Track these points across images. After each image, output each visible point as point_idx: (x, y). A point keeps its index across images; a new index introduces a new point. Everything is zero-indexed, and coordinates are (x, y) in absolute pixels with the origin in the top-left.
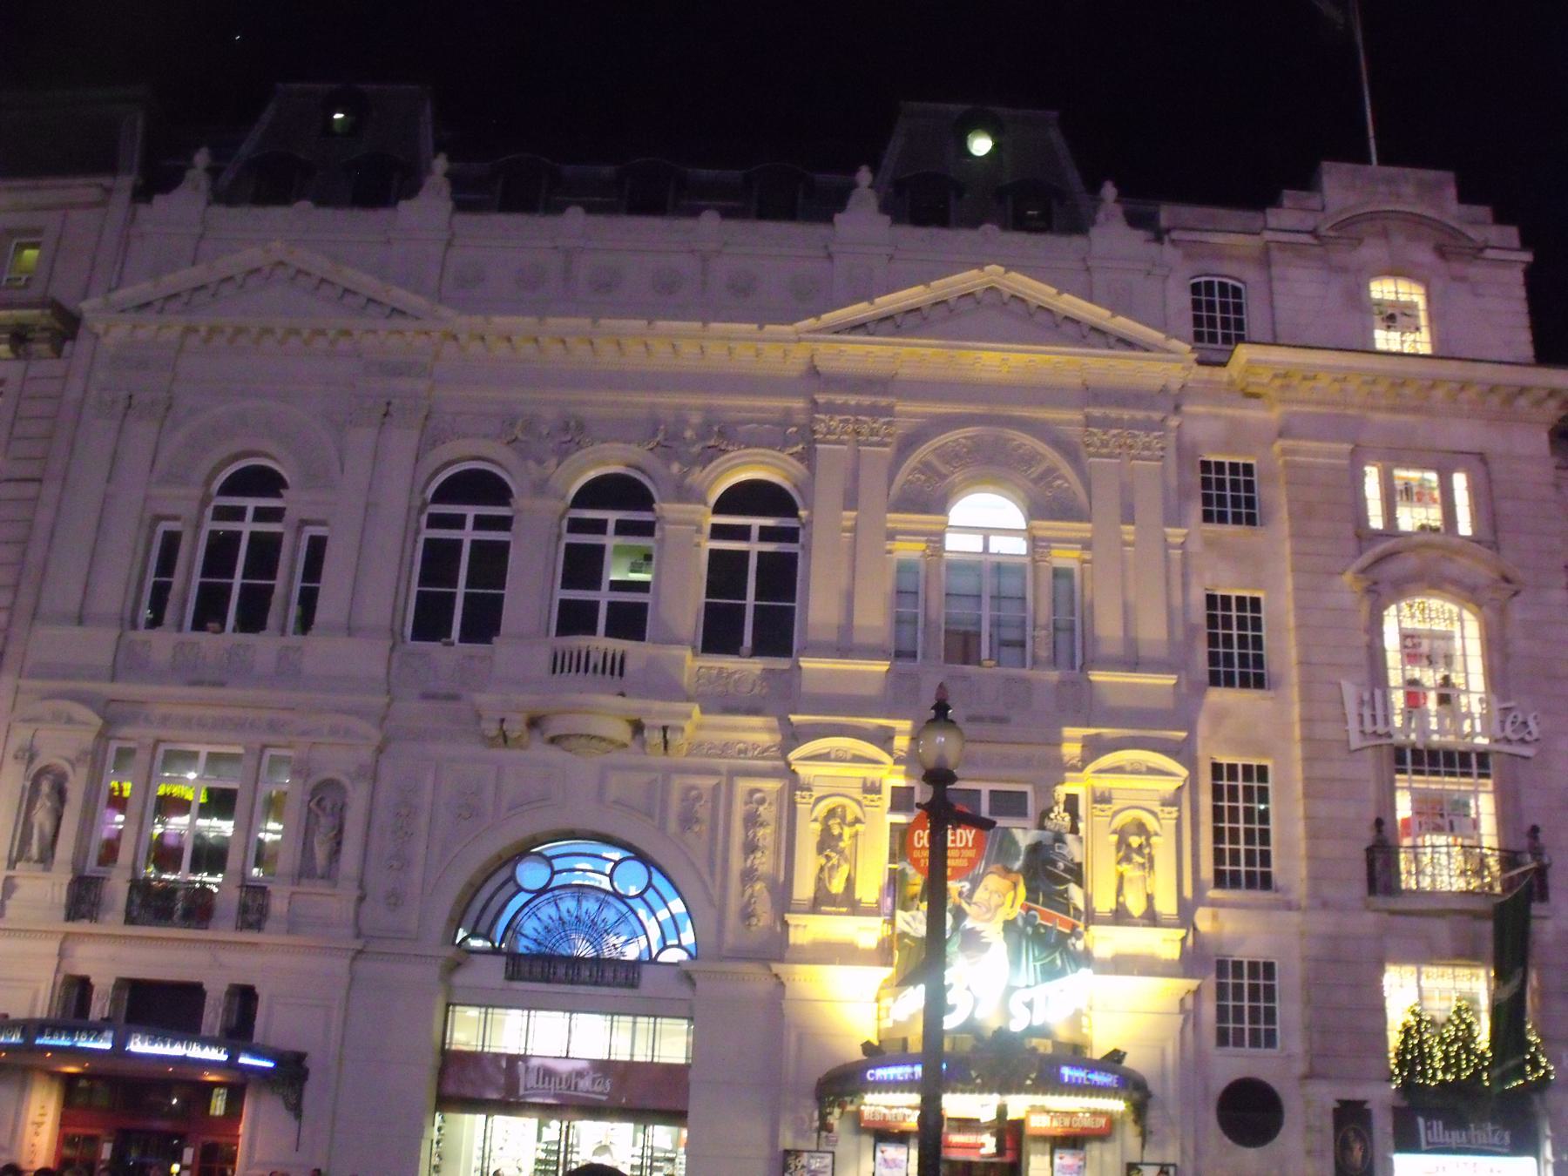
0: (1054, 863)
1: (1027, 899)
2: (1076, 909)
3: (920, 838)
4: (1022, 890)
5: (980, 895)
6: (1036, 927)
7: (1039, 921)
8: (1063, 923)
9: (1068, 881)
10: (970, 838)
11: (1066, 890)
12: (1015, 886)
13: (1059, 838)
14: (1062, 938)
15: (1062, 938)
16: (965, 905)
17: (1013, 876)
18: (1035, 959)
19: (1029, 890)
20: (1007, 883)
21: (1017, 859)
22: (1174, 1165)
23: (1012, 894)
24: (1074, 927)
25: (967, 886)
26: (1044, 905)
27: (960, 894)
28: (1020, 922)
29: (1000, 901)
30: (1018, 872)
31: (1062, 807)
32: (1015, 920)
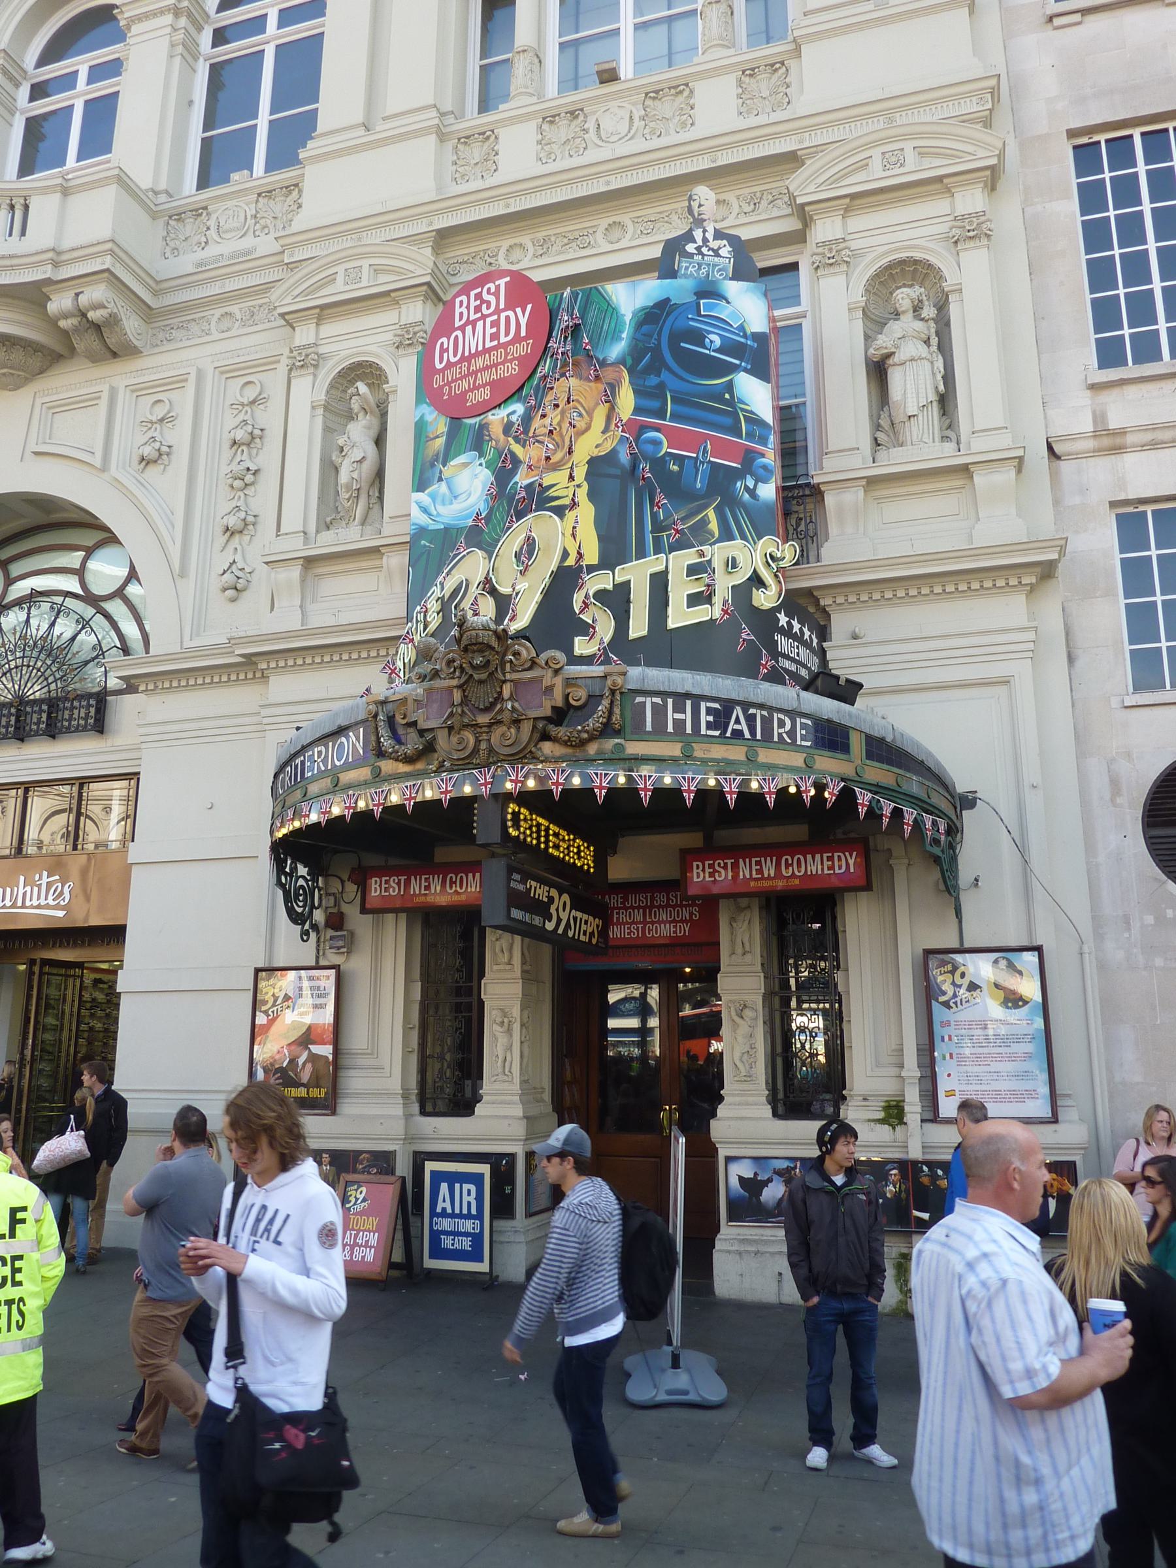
0: (698, 337)
1: (637, 410)
2: (755, 421)
3: (443, 350)
4: (626, 400)
6: (659, 464)
8: (721, 449)
9: (734, 369)
10: (523, 321)
11: (730, 386)
12: (613, 387)
13: (708, 291)
16: (517, 449)
17: (608, 374)
21: (616, 337)
25: (518, 408)
26: (675, 417)
27: (507, 428)
30: (622, 361)
32: (614, 452)
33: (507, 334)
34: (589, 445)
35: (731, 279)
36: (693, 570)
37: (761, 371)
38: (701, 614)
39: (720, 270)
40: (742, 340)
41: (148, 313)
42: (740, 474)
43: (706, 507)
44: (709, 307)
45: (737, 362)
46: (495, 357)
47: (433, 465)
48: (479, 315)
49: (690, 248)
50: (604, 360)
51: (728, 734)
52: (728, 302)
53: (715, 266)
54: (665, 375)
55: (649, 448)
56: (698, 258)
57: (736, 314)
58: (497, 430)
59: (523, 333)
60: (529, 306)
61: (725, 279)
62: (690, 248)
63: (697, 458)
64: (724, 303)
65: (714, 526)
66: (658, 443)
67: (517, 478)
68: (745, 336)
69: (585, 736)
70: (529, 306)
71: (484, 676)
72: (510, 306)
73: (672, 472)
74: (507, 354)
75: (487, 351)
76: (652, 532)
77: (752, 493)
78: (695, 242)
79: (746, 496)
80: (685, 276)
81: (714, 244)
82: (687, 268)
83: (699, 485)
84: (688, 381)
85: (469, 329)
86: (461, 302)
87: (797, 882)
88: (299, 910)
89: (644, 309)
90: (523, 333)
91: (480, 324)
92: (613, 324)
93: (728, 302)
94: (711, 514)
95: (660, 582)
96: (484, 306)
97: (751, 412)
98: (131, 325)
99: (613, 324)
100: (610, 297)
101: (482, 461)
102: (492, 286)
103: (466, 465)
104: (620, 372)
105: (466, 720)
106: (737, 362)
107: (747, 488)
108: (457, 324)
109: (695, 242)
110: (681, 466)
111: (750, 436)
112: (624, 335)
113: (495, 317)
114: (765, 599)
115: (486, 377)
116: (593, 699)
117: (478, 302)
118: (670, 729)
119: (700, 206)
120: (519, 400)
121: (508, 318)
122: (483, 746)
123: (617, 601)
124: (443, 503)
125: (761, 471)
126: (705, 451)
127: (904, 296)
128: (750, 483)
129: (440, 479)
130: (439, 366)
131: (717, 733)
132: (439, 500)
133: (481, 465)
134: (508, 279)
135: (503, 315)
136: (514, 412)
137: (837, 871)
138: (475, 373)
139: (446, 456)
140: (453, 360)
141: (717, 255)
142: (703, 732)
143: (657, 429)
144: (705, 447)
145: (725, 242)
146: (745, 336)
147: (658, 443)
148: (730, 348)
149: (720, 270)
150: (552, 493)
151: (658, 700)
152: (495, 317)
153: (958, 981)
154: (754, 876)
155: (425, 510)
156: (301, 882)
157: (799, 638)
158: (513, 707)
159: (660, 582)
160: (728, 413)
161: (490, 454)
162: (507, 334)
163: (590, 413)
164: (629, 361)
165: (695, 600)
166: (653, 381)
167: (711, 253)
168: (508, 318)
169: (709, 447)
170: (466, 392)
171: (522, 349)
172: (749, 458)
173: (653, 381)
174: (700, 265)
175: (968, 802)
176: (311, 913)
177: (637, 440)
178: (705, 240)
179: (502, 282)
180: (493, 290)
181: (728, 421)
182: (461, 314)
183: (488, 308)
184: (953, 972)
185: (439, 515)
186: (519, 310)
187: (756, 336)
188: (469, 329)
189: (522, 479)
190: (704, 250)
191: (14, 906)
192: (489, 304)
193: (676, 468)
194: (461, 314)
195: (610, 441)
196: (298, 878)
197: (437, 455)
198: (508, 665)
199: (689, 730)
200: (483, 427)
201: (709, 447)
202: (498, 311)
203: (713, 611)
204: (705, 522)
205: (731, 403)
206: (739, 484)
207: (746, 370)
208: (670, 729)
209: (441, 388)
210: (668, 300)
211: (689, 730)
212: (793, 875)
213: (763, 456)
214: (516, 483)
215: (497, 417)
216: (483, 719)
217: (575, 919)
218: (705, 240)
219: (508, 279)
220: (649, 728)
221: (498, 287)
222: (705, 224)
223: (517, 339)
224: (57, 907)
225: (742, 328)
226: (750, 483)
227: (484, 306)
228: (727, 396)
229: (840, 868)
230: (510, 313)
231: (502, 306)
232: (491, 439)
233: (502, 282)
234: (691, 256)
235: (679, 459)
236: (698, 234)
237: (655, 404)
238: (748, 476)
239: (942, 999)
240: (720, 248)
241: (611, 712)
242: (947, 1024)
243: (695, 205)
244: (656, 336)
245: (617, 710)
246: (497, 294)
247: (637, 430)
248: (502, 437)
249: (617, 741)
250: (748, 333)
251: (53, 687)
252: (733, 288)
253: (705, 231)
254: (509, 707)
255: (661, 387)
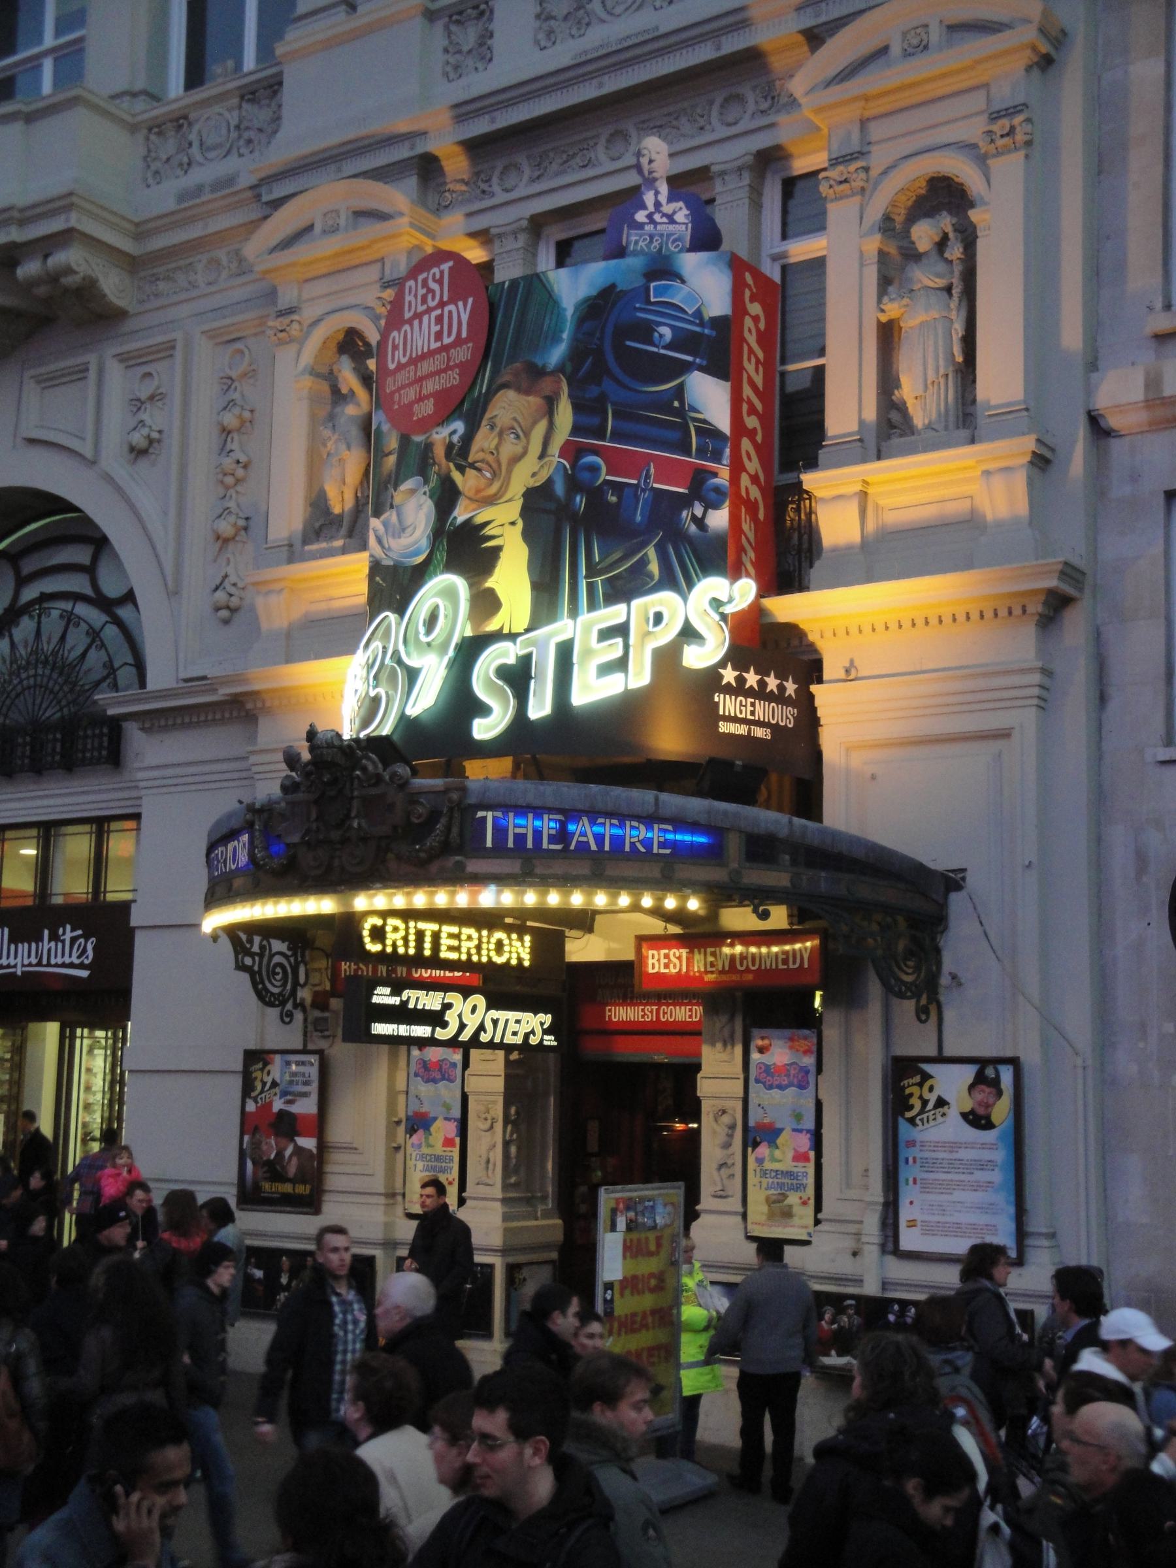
0: (646, 332)
1: (576, 430)
2: (708, 432)
4: (565, 415)
5: (484, 440)
6: (595, 495)
7: (604, 476)
8: (667, 471)
9: (686, 368)
10: (465, 318)
11: (680, 392)
12: (550, 403)
13: (662, 269)
14: (666, 510)
15: (666, 510)
16: (456, 476)
17: (546, 385)
18: (592, 571)
19: (577, 408)
20: (534, 401)
21: (556, 339)
22: (1014, 1062)
23: (542, 426)
24: (699, 478)
25: (459, 426)
26: (617, 436)
27: (450, 447)
28: (559, 489)
29: (519, 449)
30: (560, 369)
31: (664, 189)
32: (550, 482)
33: (449, 335)
34: (523, 478)
35: (690, 250)
36: (607, 634)
37: (721, 365)
38: (613, 687)
39: (674, 241)
40: (698, 329)
41: (132, 264)
42: (685, 501)
43: (644, 544)
44: (660, 291)
45: (689, 358)
46: (439, 361)
47: (386, 488)
48: (425, 307)
49: (641, 216)
50: (544, 366)
51: (572, 847)
52: (683, 282)
53: (669, 236)
54: (607, 385)
55: (585, 476)
56: (649, 228)
57: (692, 297)
58: (439, 452)
59: (464, 335)
60: (470, 300)
61: (681, 251)
62: (641, 216)
63: (637, 486)
64: (677, 284)
65: (654, 567)
66: (594, 469)
67: (455, 513)
68: (702, 324)
69: (422, 855)
70: (470, 300)
71: (332, 793)
72: (453, 300)
73: (609, 504)
74: (449, 359)
75: (431, 353)
76: (586, 577)
77: (700, 522)
78: (644, 207)
79: (693, 528)
80: (635, 253)
81: (668, 208)
82: (636, 242)
83: (639, 518)
84: (630, 389)
85: (416, 322)
86: (410, 288)
87: (750, 977)
88: (276, 991)
89: (587, 300)
90: (464, 335)
91: (425, 318)
92: (554, 322)
93: (683, 282)
94: (651, 552)
95: (565, 652)
96: (430, 296)
97: (705, 421)
98: (113, 285)
99: (554, 322)
100: (552, 287)
101: (426, 489)
102: (435, 270)
103: (413, 492)
104: (559, 382)
105: (321, 837)
106: (689, 358)
107: (694, 519)
108: (407, 315)
109: (644, 207)
110: (619, 498)
111: (702, 453)
112: (565, 336)
113: (439, 312)
114: (697, 658)
115: (431, 386)
116: (434, 816)
117: (424, 291)
118: (511, 844)
119: (651, 161)
120: (459, 418)
121: (450, 312)
122: (336, 862)
123: (518, 678)
124: (393, 536)
125: (713, 496)
126: (648, 476)
127: (924, 234)
128: (698, 510)
129: (392, 507)
130: (392, 366)
131: (559, 847)
132: (390, 530)
133: (425, 493)
134: (451, 264)
135: (446, 309)
136: (454, 432)
137: (791, 966)
138: (420, 380)
139: (397, 479)
140: (404, 360)
141: (672, 221)
142: (545, 845)
143: (595, 451)
144: (648, 471)
145: (681, 204)
146: (702, 324)
147: (594, 469)
148: (684, 341)
149: (674, 242)
150: (488, 531)
151: (499, 814)
152: (439, 312)
153: (926, 1095)
154: (709, 969)
155: (380, 541)
156: (277, 959)
157: (760, 693)
158: (359, 824)
159: (565, 652)
160: (677, 426)
161: (434, 481)
162: (449, 335)
163: (527, 434)
164: (569, 368)
165: (606, 669)
166: (593, 391)
167: (665, 220)
168: (450, 312)
169: (652, 471)
170: (411, 404)
171: (462, 354)
172: (698, 484)
173: (593, 391)
174: (651, 237)
175: (953, 882)
176: (294, 993)
177: (573, 467)
178: (658, 205)
179: (446, 267)
180: (438, 276)
181: (673, 435)
182: (410, 302)
183: (433, 298)
184: (921, 1085)
185: (389, 549)
186: (460, 304)
187: (717, 322)
188: (416, 322)
189: (461, 514)
190: (657, 217)
191: (39, 964)
192: (433, 292)
193: (614, 499)
194: (410, 302)
195: (546, 469)
196: (272, 956)
197: (390, 476)
198: (356, 782)
199: (530, 845)
200: (429, 446)
201: (652, 471)
202: (442, 304)
203: (640, 676)
204: (644, 562)
205: (681, 412)
206: (684, 514)
207: (701, 369)
208: (511, 844)
209: (393, 393)
210: (613, 286)
211: (530, 845)
212: (748, 970)
213: (715, 475)
214: (455, 518)
215: (440, 436)
216: (335, 835)
217: (495, 1022)
218: (658, 205)
219: (451, 264)
220: (489, 844)
221: (442, 272)
222: (658, 184)
223: (459, 342)
224: (81, 966)
225: (698, 313)
226: (698, 510)
227: (430, 296)
228: (676, 404)
229: (794, 962)
230: (452, 307)
231: (445, 298)
232: (434, 463)
233: (446, 267)
234: (640, 226)
235: (618, 488)
236: (649, 198)
237: (595, 421)
238: (697, 503)
239: (908, 1115)
240: (675, 212)
241: (448, 829)
242: (911, 1143)
243: (644, 161)
244: (598, 335)
245: (455, 830)
246: (440, 282)
247: (572, 451)
248: (444, 461)
249: (458, 858)
250: (706, 318)
251: (66, 711)
252: (691, 263)
253: (657, 193)
254: (355, 825)
255: (602, 400)
